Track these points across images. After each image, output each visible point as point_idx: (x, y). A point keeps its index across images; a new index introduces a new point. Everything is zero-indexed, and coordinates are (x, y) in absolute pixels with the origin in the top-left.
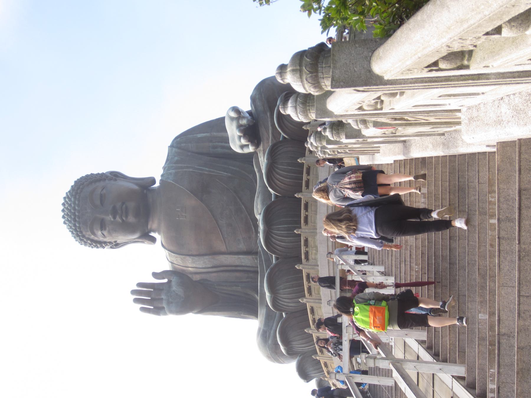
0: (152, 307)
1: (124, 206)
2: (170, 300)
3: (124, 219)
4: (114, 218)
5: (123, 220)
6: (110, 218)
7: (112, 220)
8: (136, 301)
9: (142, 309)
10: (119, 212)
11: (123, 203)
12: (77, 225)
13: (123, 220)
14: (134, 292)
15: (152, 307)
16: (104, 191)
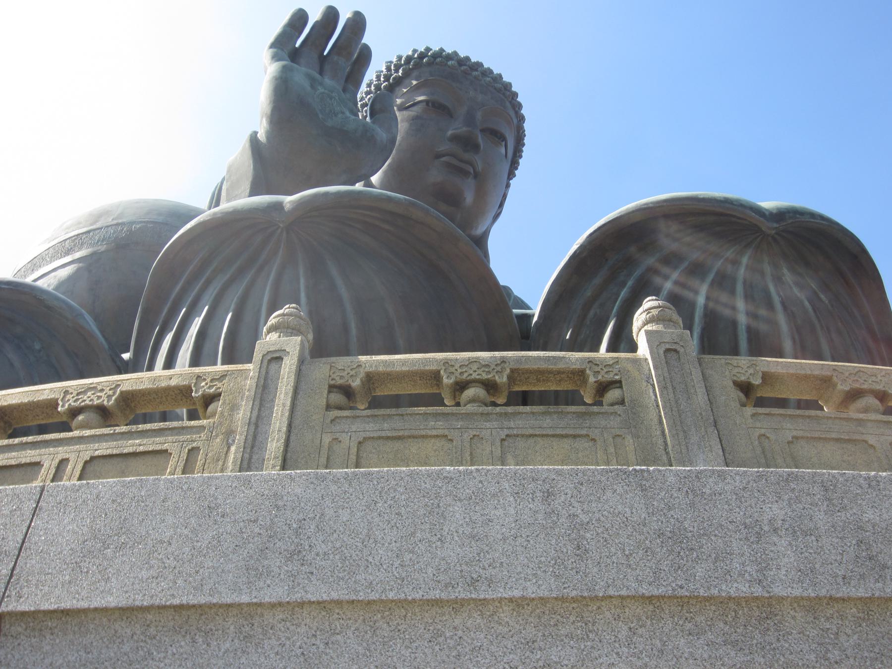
0: (297, 45)
1: (472, 171)
2: (321, 90)
3: (444, 159)
4: (455, 139)
5: (438, 156)
6: (456, 128)
7: (450, 133)
8: (331, 15)
9: (300, 18)
10: (467, 156)
11: (476, 175)
12: (450, 63)
13: (438, 156)
14: (358, 23)
15: (298, 45)
16: (503, 150)
